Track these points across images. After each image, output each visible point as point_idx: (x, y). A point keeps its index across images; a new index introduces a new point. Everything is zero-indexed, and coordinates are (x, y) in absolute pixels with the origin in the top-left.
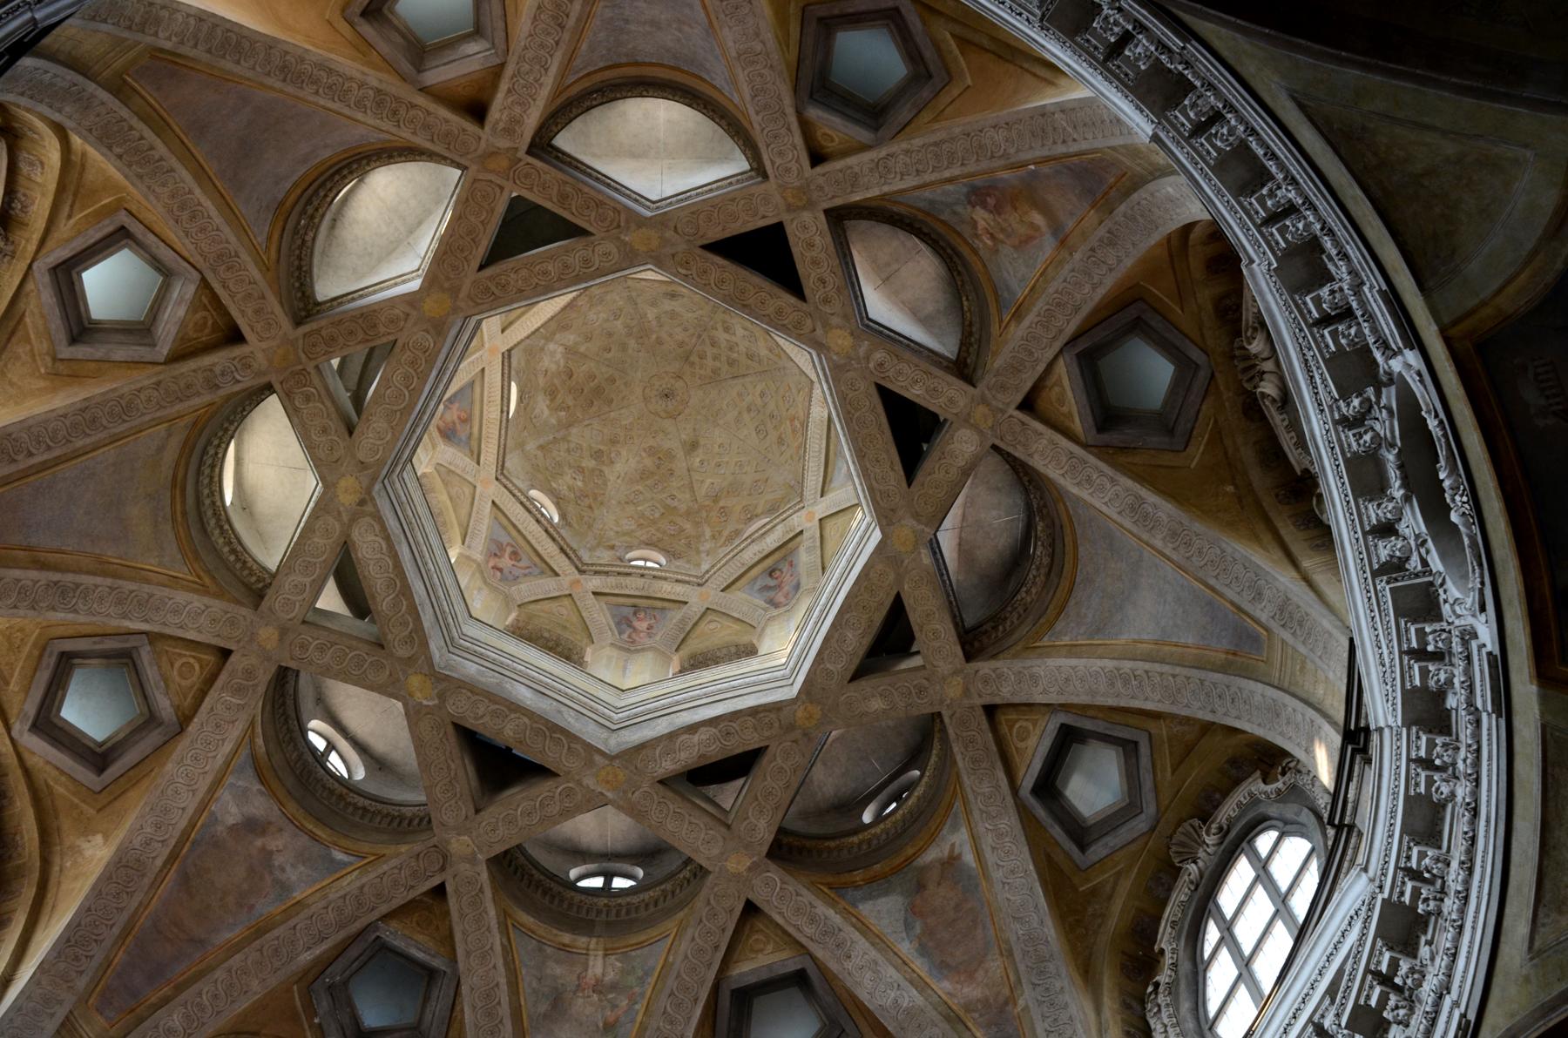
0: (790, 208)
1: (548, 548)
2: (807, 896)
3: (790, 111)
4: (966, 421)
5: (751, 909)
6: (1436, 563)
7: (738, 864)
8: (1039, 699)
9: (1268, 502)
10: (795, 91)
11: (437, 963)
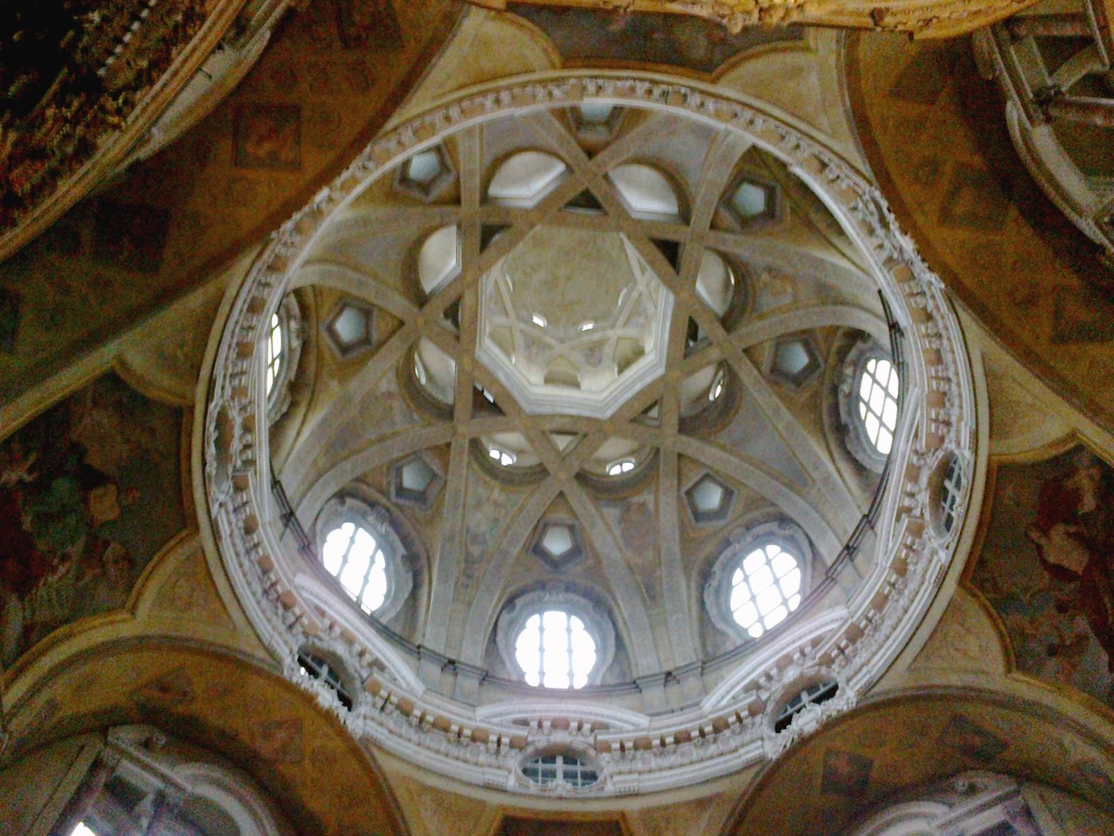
0: (691, 240)
1: (509, 305)
2: (585, 498)
3: (714, 206)
4: (719, 345)
5: (561, 494)
6: (927, 515)
7: (562, 475)
8: (702, 459)
9: (827, 427)
10: (720, 199)
11: (440, 473)
